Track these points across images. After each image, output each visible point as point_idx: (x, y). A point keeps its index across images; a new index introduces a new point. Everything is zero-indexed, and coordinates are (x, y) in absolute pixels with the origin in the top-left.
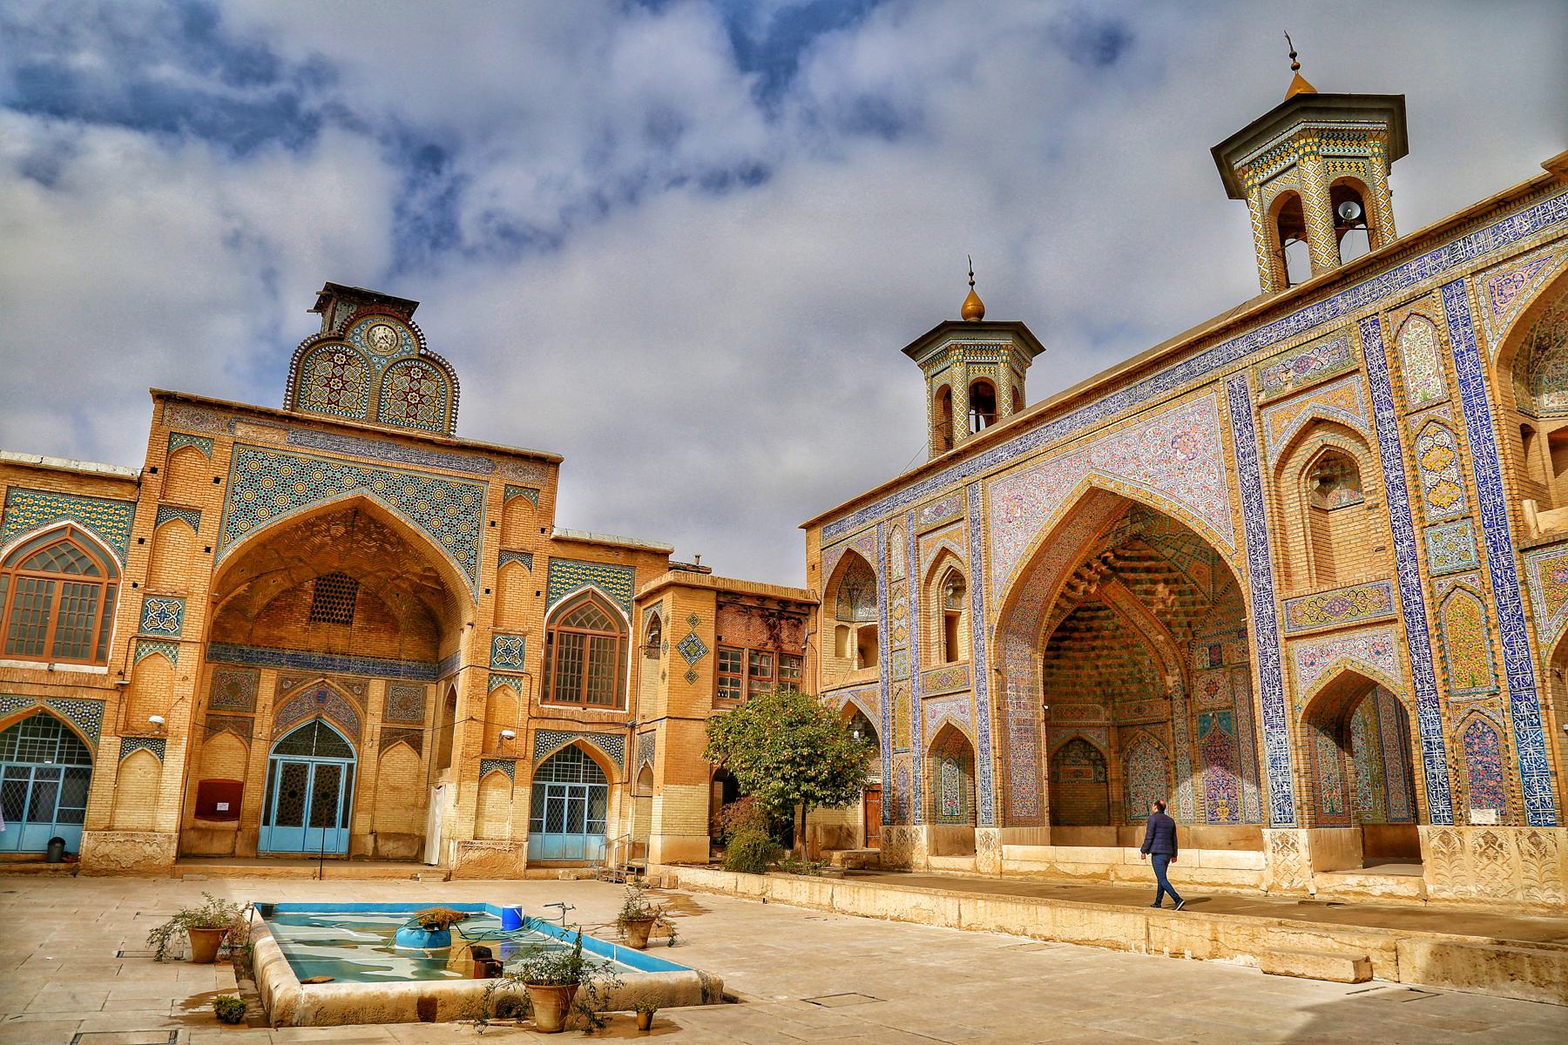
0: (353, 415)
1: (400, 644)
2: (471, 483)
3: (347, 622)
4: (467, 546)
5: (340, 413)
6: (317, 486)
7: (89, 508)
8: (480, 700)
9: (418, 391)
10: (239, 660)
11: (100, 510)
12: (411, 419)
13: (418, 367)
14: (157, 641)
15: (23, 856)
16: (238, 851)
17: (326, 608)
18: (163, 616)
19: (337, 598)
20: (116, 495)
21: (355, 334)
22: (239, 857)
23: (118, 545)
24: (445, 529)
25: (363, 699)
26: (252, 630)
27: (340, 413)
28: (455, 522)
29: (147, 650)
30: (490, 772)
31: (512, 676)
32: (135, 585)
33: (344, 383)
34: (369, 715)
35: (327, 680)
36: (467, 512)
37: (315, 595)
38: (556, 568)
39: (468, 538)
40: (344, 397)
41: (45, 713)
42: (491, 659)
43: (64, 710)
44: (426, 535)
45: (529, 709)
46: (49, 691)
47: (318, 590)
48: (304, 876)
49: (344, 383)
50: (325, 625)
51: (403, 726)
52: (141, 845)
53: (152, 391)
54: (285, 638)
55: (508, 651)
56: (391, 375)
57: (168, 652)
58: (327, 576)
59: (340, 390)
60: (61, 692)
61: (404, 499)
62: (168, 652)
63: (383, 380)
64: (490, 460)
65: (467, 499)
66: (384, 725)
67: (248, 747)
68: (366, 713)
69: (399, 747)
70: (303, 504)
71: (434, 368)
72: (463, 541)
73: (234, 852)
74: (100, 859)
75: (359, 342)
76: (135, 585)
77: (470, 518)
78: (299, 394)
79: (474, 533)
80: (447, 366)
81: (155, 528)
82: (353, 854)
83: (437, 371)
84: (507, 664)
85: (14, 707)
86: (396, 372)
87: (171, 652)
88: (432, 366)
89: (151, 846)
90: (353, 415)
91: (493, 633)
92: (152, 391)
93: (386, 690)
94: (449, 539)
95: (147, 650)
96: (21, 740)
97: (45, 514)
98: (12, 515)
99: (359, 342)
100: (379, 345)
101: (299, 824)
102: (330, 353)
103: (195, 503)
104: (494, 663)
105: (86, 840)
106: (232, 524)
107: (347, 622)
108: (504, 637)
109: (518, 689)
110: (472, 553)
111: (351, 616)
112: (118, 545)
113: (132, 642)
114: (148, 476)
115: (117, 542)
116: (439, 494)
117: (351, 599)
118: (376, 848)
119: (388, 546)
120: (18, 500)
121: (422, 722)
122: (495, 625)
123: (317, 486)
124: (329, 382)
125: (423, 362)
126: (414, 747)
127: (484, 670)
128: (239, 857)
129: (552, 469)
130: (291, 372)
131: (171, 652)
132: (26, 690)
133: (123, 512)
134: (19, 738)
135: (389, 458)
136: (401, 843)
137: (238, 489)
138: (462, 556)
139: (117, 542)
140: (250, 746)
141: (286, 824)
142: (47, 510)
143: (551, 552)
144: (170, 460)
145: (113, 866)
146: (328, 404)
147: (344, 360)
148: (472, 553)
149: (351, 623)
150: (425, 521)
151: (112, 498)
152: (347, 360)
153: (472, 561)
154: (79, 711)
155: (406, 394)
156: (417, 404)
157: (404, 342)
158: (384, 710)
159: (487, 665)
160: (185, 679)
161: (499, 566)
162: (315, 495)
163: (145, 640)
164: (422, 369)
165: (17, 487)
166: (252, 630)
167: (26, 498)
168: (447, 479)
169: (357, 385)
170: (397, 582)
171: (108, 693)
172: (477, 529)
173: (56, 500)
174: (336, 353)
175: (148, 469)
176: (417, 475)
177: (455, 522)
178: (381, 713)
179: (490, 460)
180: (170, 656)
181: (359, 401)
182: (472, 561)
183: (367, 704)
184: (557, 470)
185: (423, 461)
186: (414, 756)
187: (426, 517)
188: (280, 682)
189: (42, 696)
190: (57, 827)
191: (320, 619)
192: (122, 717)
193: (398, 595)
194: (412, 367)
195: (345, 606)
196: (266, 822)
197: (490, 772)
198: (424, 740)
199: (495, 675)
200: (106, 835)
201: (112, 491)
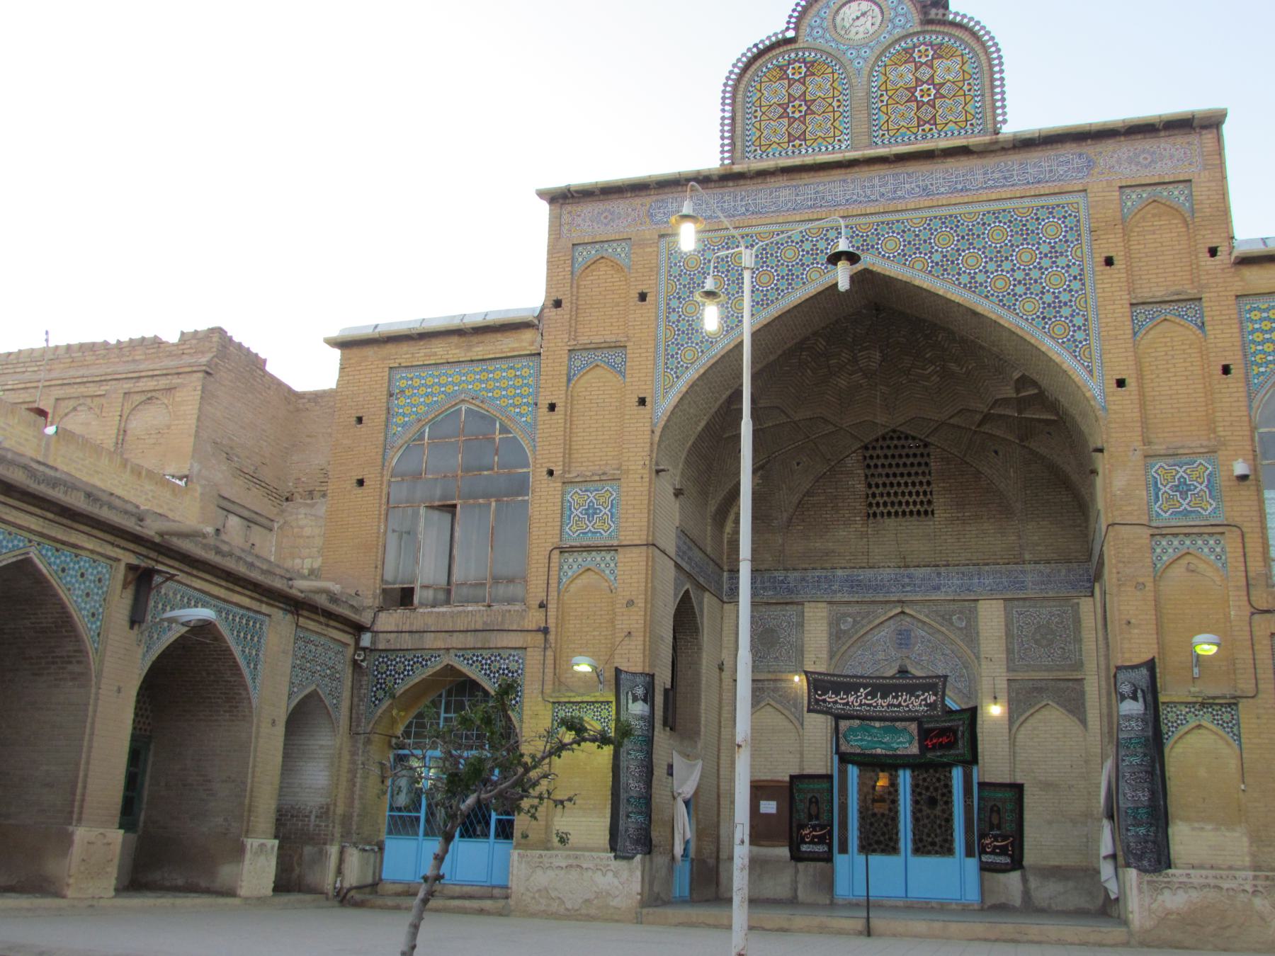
0: (830, 148)
1: (1020, 537)
2: (1052, 201)
3: (926, 513)
4: (1066, 311)
5: (810, 150)
6: (790, 270)
7: (484, 376)
8: (1140, 586)
9: (931, 80)
10: (770, 593)
11: (498, 375)
12: (927, 127)
13: (924, 44)
14: (588, 549)
15: (457, 888)
16: (801, 895)
17: (889, 494)
18: (591, 512)
19: (902, 475)
20: (513, 350)
21: (812, 28)
22: (803, 904)
23: (524, 419)
24: (1020, 289)
25: (971, 635)
26: (783, 545)
27: (810, 150)
28: (1035, 274)
29: (575, 566)
30: (1185, 729)
31: (1201, 534)
32: (551, 473)
33: (809, 104)
34: (983, 662)
35: (907, 611)
36: (1054, 253)
37: (866, 476)
38: (1255, 315)
39: (1065, 297)
40: (814, 125)
41: (450, 670)
42: (1150, 510)
43: (477, 667)
44: (985, 307)
45: (1248, 594)
46: (456, 641)
47: (868, 466)
48: (840, 932)
49: (809, 104)
50: (891, 523)
51: (1045, 675)
52: (590, 873)
53: (542, 194)
54: (833, 551)
55: (1183, 488)
56: (882, 69)
57: (603, 565)
58: (877, 440)
59: (789, 102)
60: (470, 641)
61: (936, 257)
62: (603, 565)
63: (869, 81)
64: (1080, 155)
65: (1052, 230)
66: (1013, 676)
67: (799, 727)
68: (978, 658)
69: (1045, 712)
70: (772, 302)
71: (951, 36)
72: (1057, 304)
73: (796, 897)
74: (537, 895)
75: (822, 37)
76: (551, 473)
77: (1062, 261)
78: (744, 140)
79: (1076, 285)
80: (977, 28)
81: (568, 387)
82: (989, 903)
83: (951, 36)
84: (1186, 513)
85: (417, 668)
86: (888, 63)
87: (608, 565)
88: (947, 34)
89: (604, 875)
90: (830, 148)
91: (1146, 457)
92: (542, 194)
93: (1006, 617)
94: (1029, 306)
95: (575, 566)
96: (446, 719)
97: (433, 394)
98: (399, 406)
99: (822, 37)
100: (853, 30)
101: (949, 851)
102: (781, 68)
103: (608, 335)
104: (1158, 514)
105: (516, 864)
106: (672, 356)
107: (926, 513)
108: (1171, 461)
109: (1218, 557)
110: (1078, 321)
111: (929, 502)
112: (524, 419)
113: (552, 556)
114: (552, 313)
115: (522, 415)
116: (998, 235)
117: (924, 474)
118: (1026, 893)
119: (953, 367)
120: (403, 384)
121: (1079, 665)
122: (1147, 442)
123: (790, 270)
124: (785, 110)
125: (932, 32)
126: (1070, 711)
127: (1138, 529)
128: (803, 904)
129: (1208, 137)
130: (723, 111)
131: (608, 565)
132: (430, 641)
133: (525, 372)
134: (443, 715)
135: (900, 198)
136: (1071, 884)
137: (674, 303)
138: (1058, 330)
139: (522, 415)
140: (802, 724)
141: (929, 853)
142: (436, 389)
143: (1238, 287)
144: (578, 287)
145: (554, 907)
146: (789, 142)
147: (804, 70)
148: (1078, 321)
149: (933, 513)
150: (981, 285)
151: (509, 354)
152: (808, 69)
153: (1080, 336)
154: (495, 667)
155: (912, 90)
156: (934, 100)
157: (893, 13)
158: (1009, 651)
159: (1144, 520)
160: (630, 603)
161: (1135, 334)
162: (790, 284)
163: (572, 550)
164: (931, 44)
165: (400, 366)
166: (783, 545)
167: (411, 379)
168: (1008, 205)
169: (830, 101)
170: (986, 428)
171: (529, 637)
172: (1079, 277)
173: (446, 374)
174: (789, 64)
175: (550, 304)
176: (954, 211)
177: (1035, 274)
178: (1005, 656)
179: (1080, 155)
180: (607, 572)
181: (837, 124)
182: (1080, 336)
183: (979, 644)
184: (1219, 139)
185: (960, 187)
186: (1076, 728)
187: (980, 278)
188: (834, 623)
189: (448, 649)
190: (496, 845)
191: (882, 515)
192: (549, 670)
193: (996, 452)
194: (915, 46)
195: (921, 497)
196: (844, 849)
197: (1185, 729)
198: (1087, 696)
199: (1163, 535)
200: (541, 856)
201: (508, 344)
